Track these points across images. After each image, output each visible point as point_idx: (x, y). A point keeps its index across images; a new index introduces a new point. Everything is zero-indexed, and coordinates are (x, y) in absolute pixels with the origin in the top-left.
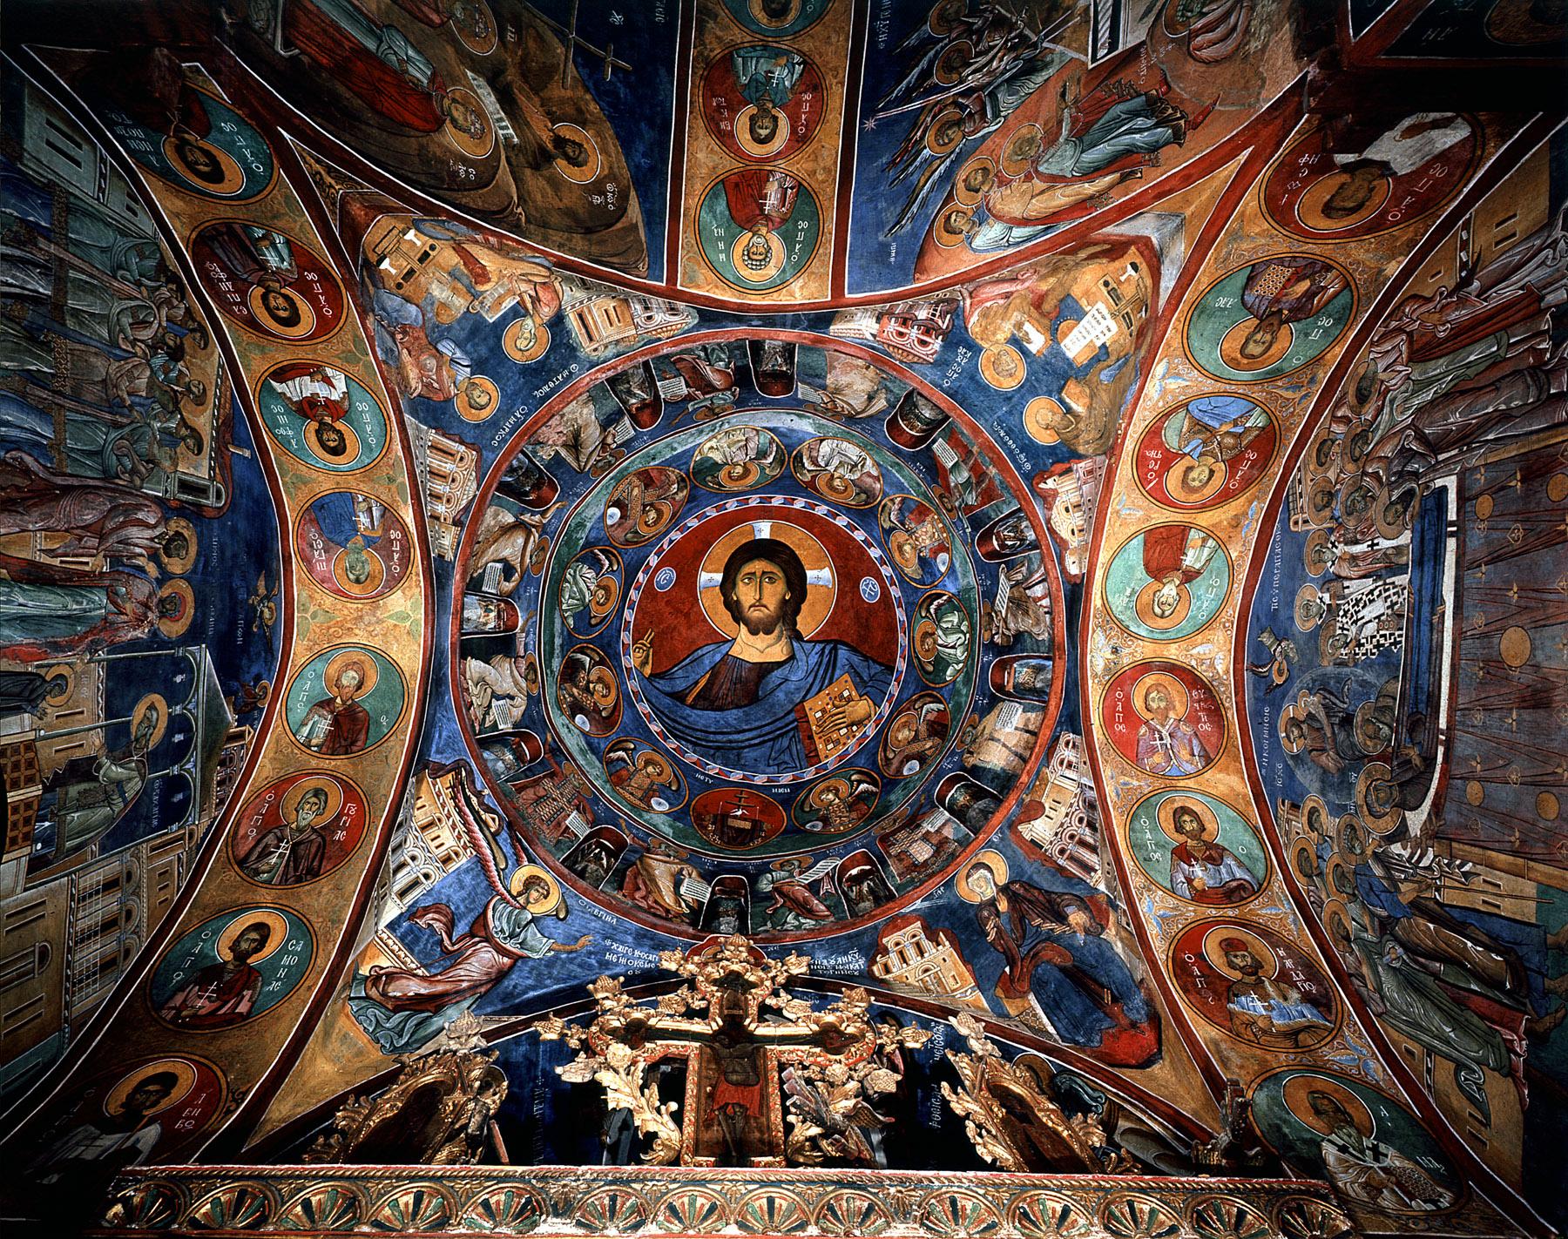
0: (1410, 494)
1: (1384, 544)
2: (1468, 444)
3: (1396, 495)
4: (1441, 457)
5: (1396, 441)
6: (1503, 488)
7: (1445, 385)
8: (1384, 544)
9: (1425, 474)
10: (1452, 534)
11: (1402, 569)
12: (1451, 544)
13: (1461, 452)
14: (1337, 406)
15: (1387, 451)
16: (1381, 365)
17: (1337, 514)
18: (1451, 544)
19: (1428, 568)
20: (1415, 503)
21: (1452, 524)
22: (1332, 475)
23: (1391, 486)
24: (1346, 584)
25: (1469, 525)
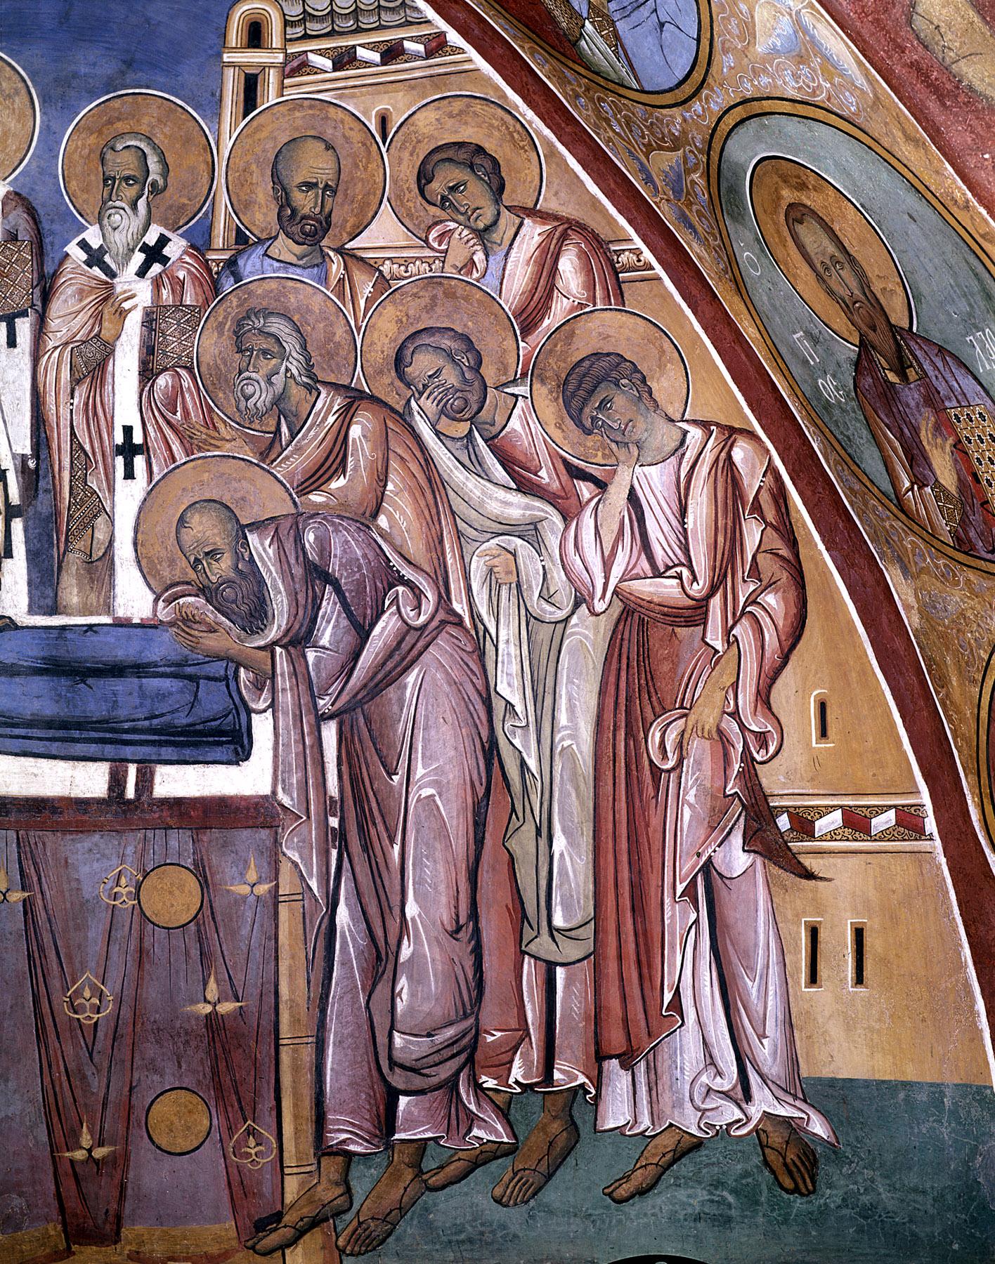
0: (257, 616)
1: (127, 498)
2: (341, 836)
3: (261, 547)
4: (330, 733)
5: (416, 547)
6: (205, 956)
7: (520, 744)
8: (127, 498)
9: (299, 672)
10: (117, 782)
11: (45, 592)
12: (89, 780)
13: (329, 807)
14: (599, 249)
15: (400, 516)
16: (656, 481)
17: (251, 265)
18: (89, 780)
19: (35, 698)
20: (225, 637)
21: (145, 781)
22: (383, 234)
23: (287, 530)
24: (24, 327)
25: (131, 843)
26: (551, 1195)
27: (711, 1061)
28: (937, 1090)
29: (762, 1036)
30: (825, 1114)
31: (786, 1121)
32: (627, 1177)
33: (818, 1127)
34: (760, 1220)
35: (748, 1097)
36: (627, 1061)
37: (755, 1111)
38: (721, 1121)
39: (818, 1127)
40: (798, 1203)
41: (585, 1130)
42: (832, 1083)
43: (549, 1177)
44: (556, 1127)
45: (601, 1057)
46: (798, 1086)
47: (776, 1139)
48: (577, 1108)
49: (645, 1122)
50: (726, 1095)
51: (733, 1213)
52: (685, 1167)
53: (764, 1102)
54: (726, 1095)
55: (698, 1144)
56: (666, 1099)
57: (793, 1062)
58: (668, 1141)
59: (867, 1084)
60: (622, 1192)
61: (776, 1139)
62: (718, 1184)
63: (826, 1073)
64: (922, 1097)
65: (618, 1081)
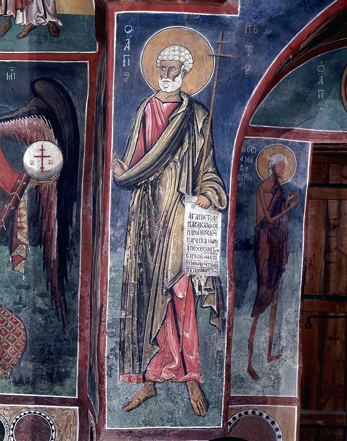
26: (6, 37)
27: (39, 11)
28: (84, 16)
29: (49, 5)
30: (61, 21)
31: (54, 22)
32: (21, 33)
33: (60, 24)
34: (47, 42)
35: (46, 17)
36: (22, 11)
37: (47, 20)
38: (40, 23)
39: (60, 24)
40: (55, 39)
41: (13, 24)
42: (63, 15)
43: (5, 33)
44: (7, 23)
45: (16, 9)
46: (56, 15)
47: (51, 26)
48: (11, 20)
49: (25, 22)
50: (42, 17)
51: (42, 41)
52: (33, 32)
53: (49, 19)
54: (42, 17)
55: (36, 27)
56: (30, 17)
57: (55, 11)
58: (30, 26)
59: (70, 15)
60: (20, 36)
61: (51, 26)
62: (39, 35)
63: (62, 13)
64: (81, 18)
65: (20, 14)
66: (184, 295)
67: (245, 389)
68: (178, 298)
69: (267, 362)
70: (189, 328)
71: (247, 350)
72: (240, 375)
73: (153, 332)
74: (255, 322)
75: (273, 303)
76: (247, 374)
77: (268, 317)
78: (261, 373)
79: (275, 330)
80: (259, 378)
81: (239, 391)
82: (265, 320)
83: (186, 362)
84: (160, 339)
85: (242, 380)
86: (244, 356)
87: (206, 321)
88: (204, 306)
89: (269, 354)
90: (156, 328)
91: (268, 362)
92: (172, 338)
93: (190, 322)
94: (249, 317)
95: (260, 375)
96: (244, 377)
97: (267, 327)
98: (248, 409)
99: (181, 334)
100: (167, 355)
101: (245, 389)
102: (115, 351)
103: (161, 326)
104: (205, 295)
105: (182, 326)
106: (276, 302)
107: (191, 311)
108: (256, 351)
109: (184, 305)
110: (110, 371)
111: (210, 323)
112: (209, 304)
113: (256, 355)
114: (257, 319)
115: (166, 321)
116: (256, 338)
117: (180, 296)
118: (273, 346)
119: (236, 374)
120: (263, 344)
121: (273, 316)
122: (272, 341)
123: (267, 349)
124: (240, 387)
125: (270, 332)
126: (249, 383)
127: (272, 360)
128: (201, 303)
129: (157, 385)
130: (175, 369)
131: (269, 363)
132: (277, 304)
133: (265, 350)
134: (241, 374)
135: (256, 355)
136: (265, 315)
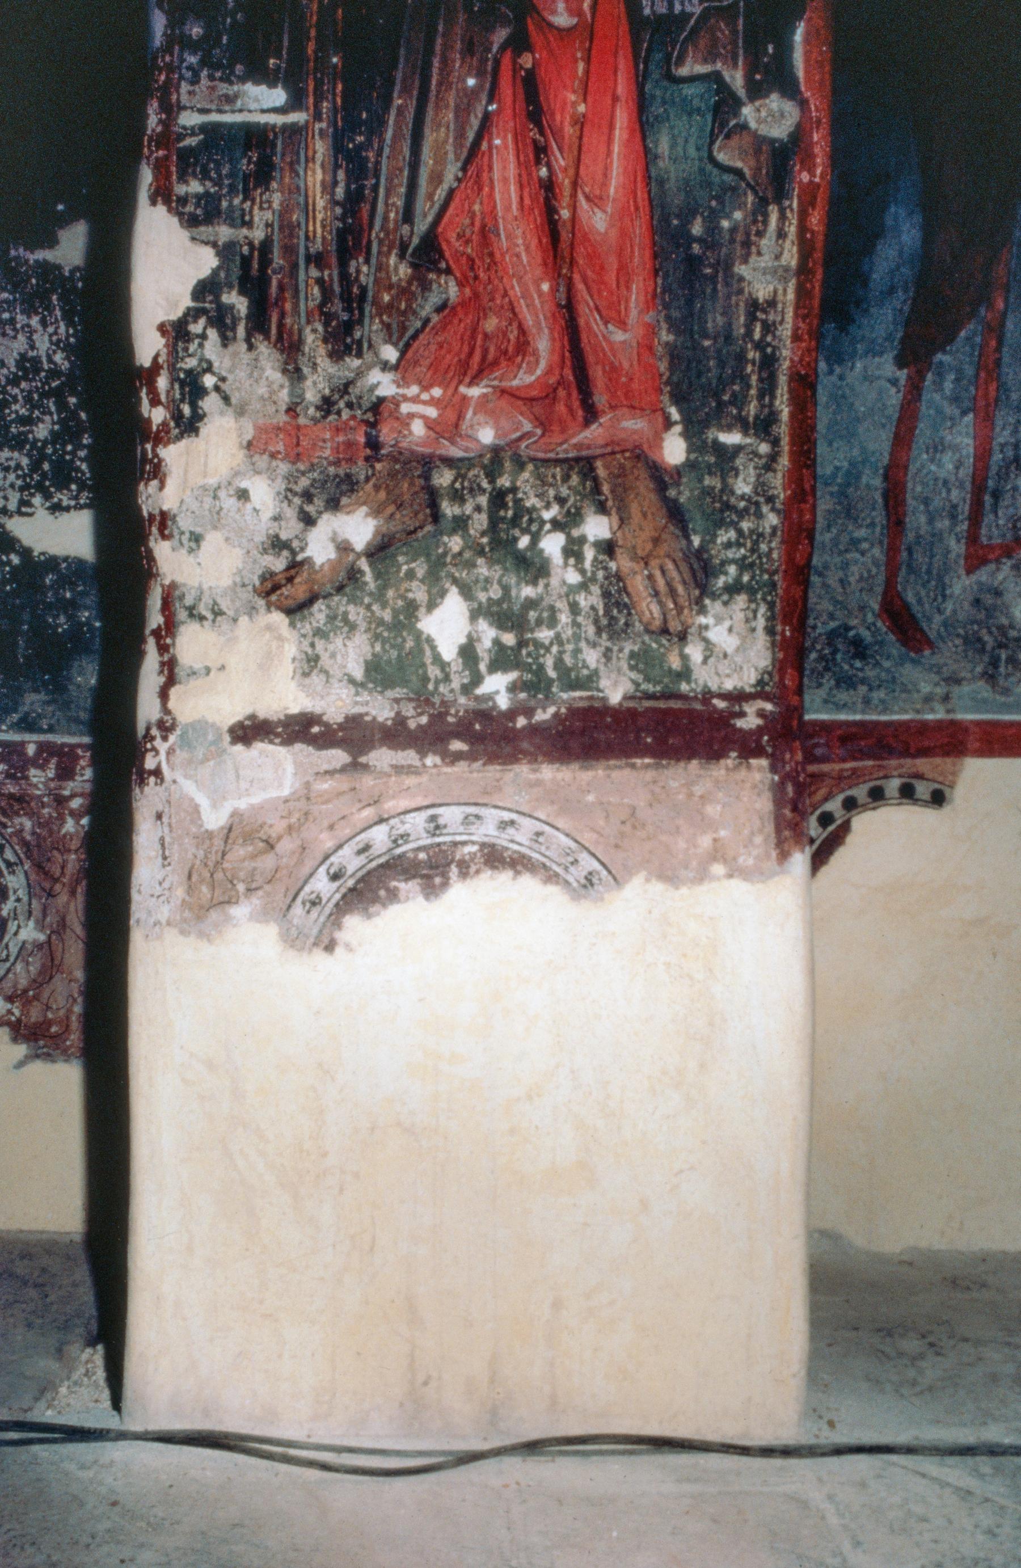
66: (579, 13)
67: (871, 689)
68: (550, 25)
69: (962, 572)
70: (605, 185)
71: (879, 516)
72: (848, 628)
73: (421, 204)
74: (914, 390)
75: (991, 306)
76: (879, 624)
77: (969, 371)
78: (938, 619)
79: (998, 429)
80: (930, 644)
81: (843, 696)
82: (957, 380)
83: (591, 358)
84: (451, 242)
85: (859, 650)
86: (865, 545)
87: (692, 152)
88: (684, 71)
89: (972, 538)
90: (437, 178)
91: (969, 572)
92: (518, 241)
93: (609, 153)
94: (886, 366)
95: (933, 627)
96: (866, 635)
97: (964, 413)
98: (886, 777)
99: (565, 214)
100: (491, 324)
101: (871, 689)
102: (217, 300)
103: (464, 169)
104: (685, 16)
105: (571, 172)
106: (1000, 305)
107: (615, 99)
108: (917, 520)
109: (581, 66)
110: (194, 406)
111: (712, 159)
112: (705, 61)
113: (918, 537)
114: (921, 375)
115: (484, 146)
116: (919, 458)
117: (562, 19)
118: (987, 499)
119: (833, 624)
120: (949, 491)
121: (989, 368)
122: (985, 479)
123: (965, 509)
124: (847, 682)
125: (975, 438)
126: (887, 664)
127: (984, 561)
128: (668, 58)
129: (444, 478)
130: (534, 393)
131: (974, 578)
132: (1004, 314)
133: (953, 517)
134: (853, 622)
135: (918, 537)
136: (956, 358)
